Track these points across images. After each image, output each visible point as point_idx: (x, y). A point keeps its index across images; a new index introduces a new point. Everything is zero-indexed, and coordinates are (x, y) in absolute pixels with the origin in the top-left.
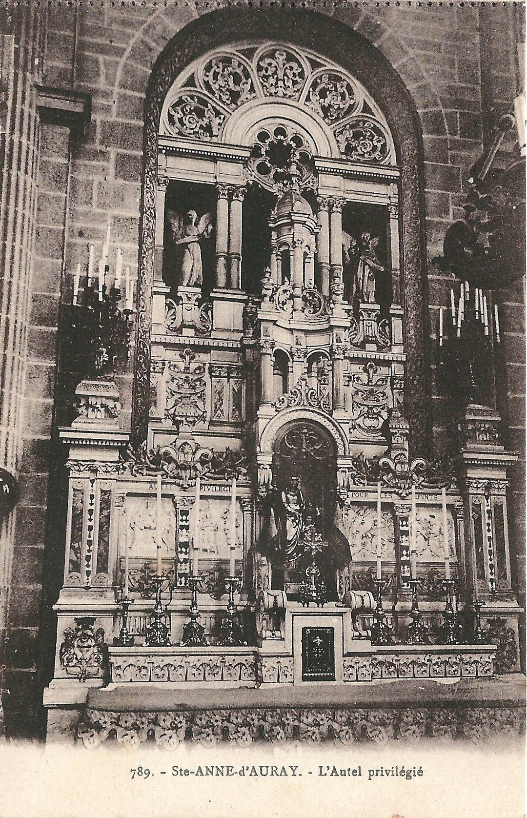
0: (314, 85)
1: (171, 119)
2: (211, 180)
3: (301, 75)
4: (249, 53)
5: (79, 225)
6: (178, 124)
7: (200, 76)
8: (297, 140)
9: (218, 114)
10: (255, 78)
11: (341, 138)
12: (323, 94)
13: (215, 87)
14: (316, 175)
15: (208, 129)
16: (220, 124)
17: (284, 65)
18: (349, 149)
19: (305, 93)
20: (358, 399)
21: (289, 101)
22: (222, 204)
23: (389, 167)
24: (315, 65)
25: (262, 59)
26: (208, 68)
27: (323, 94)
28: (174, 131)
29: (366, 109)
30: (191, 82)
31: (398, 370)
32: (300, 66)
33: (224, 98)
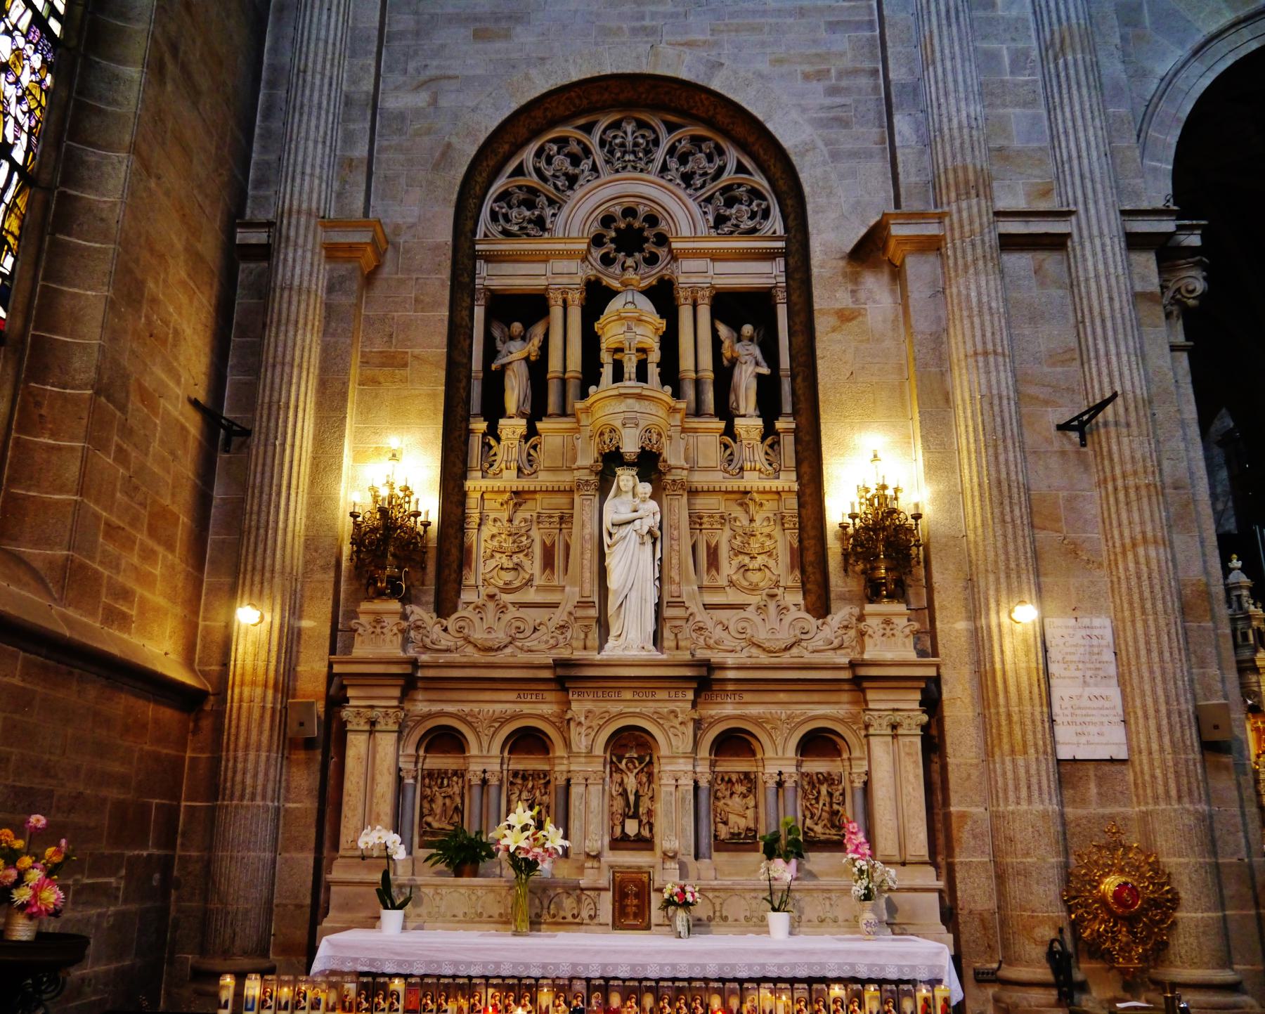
0: (672, 151)
1: (494, 216)
2: (543, 282)
3: (656, 142)
4: (588, 129)
5: (417, 351)
6: (502, 221)
7: (529, 165)
8: (652, 220)
9: (551, 202)
10: (599, 156)
11: (710, 208)
12: (683, 160)
13: (548, 174)
14: (674, 258)
15: (540, 223)
16: (554, 215)
17: (633, 132)
18: (720, 220)
19: (658, 164)
20: (737, 542)
21: (644, 176)
22: (556, 312)
23: (774, 238)
24: (671, 128)
25: (604, 132)
26: (539, 154)
27: (683, 160)
28: (495, 229)
29: (741, 168)
30: (519, 171)
31: (793, 503)
32: (654, 131)
33: (559, 184)
